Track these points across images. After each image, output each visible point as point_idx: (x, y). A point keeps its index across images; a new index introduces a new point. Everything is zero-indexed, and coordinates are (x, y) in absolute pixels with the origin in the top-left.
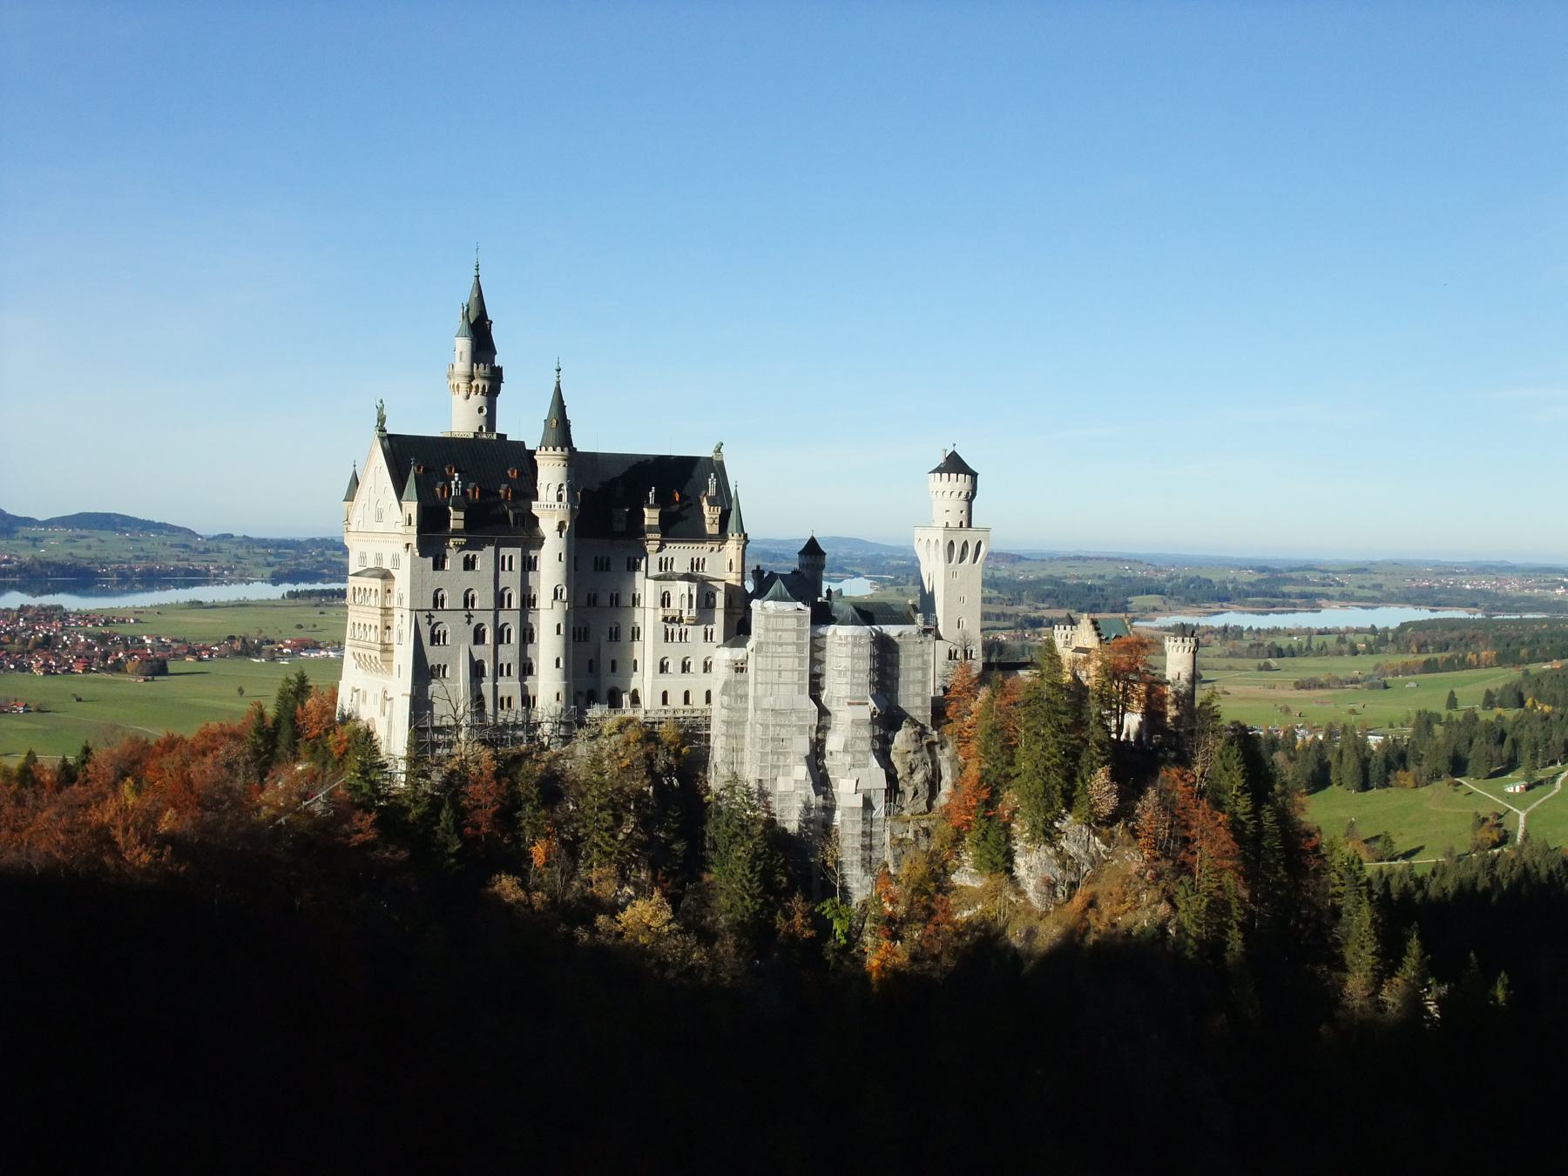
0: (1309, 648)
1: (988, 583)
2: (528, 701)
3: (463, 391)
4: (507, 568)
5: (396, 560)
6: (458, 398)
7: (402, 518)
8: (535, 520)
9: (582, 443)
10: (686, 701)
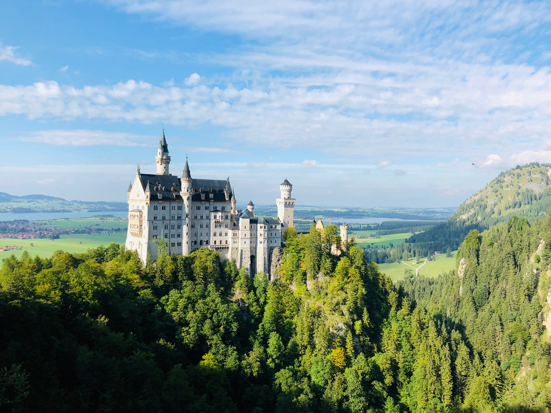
0: (360, 228)
1: (295, 212)
2: (180, 244)
3: (160, 163)
4: (173, 209)
5: (143, 207)
6: (159, 165)
7: (145, 196)
8: (181, 197)
9: (194, 175)
10: (221, 244)
